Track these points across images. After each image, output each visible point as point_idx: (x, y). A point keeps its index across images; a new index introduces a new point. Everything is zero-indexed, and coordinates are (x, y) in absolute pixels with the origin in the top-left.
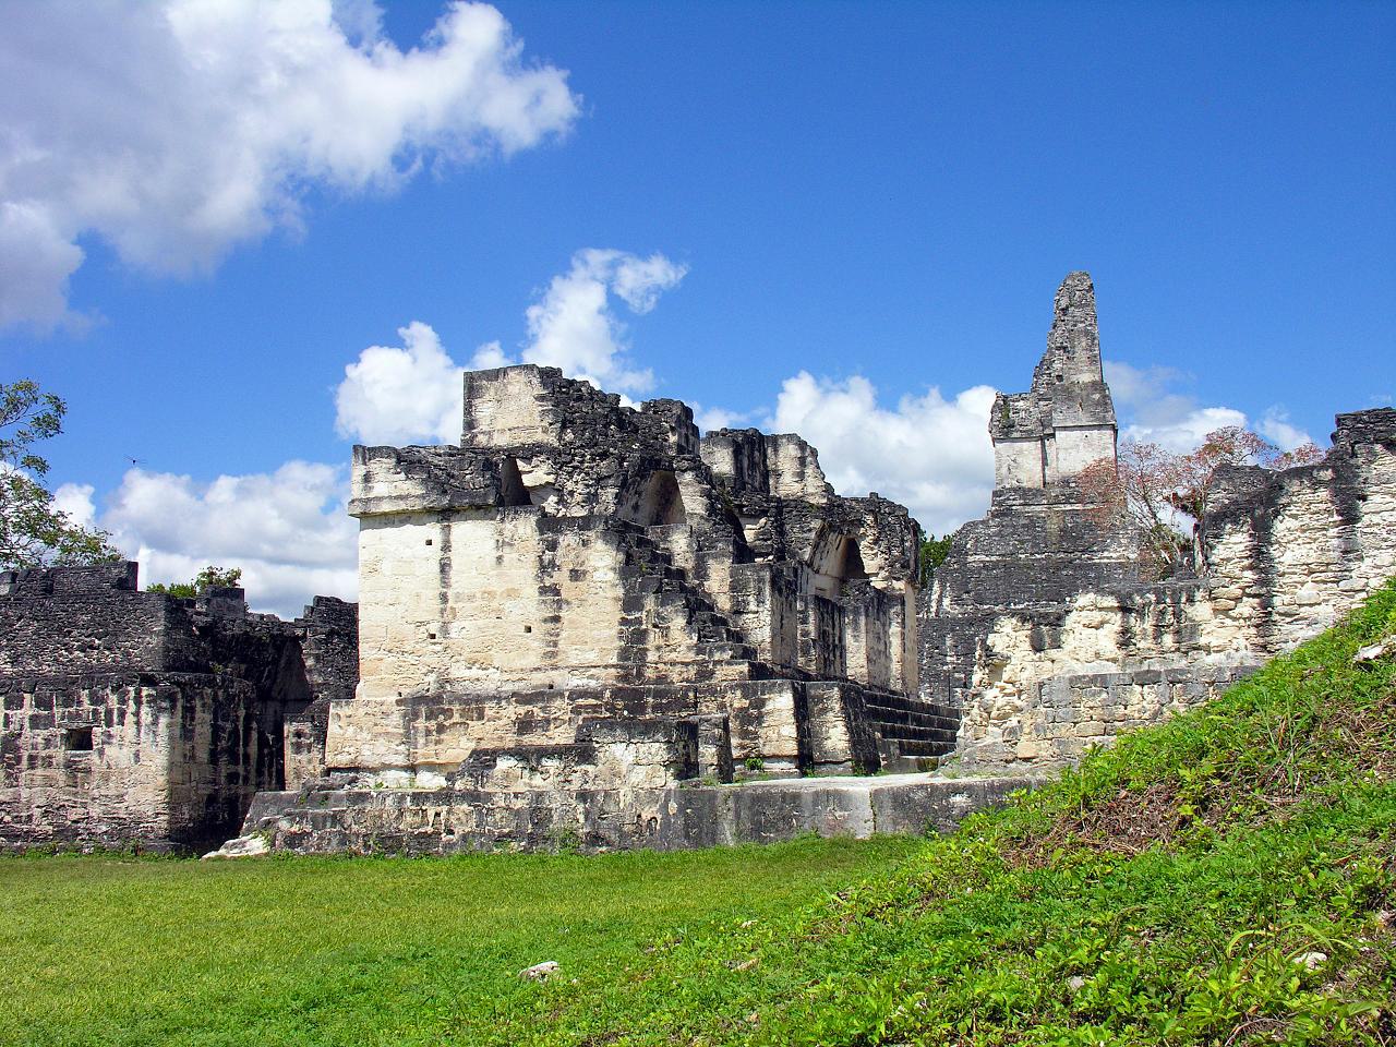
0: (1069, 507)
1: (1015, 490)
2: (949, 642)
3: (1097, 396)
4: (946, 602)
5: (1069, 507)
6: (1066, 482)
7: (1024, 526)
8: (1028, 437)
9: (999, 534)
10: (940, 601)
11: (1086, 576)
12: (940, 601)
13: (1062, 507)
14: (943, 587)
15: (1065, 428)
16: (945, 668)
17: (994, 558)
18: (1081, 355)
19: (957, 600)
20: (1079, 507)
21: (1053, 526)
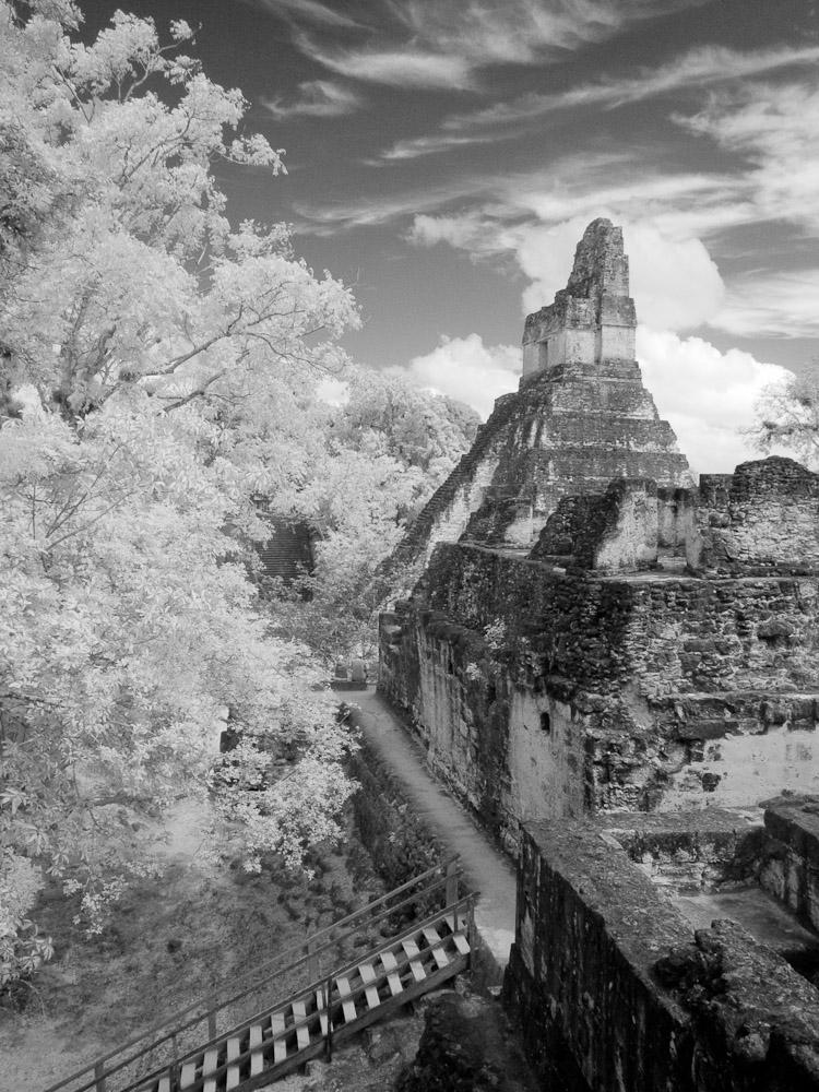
0: (609, 380)
1: (579, 364)
2: (551, 465)
3: (628, 307)
4: (544, 438)
5: (609, 380)
6: (607, 363)
7: (587, 390)
8: (588, 327)
9: (572, 394)
10: (539, 434)
11: (628, 427)
12: (539, 434)
13: (605, 379)
14: (541, 425)
15: (608, 326)
16: (549, 483)
17: (569, 410)
18: (619, 278)
19: (551, 437)
20: (615, 380)
21: (604, 391)
